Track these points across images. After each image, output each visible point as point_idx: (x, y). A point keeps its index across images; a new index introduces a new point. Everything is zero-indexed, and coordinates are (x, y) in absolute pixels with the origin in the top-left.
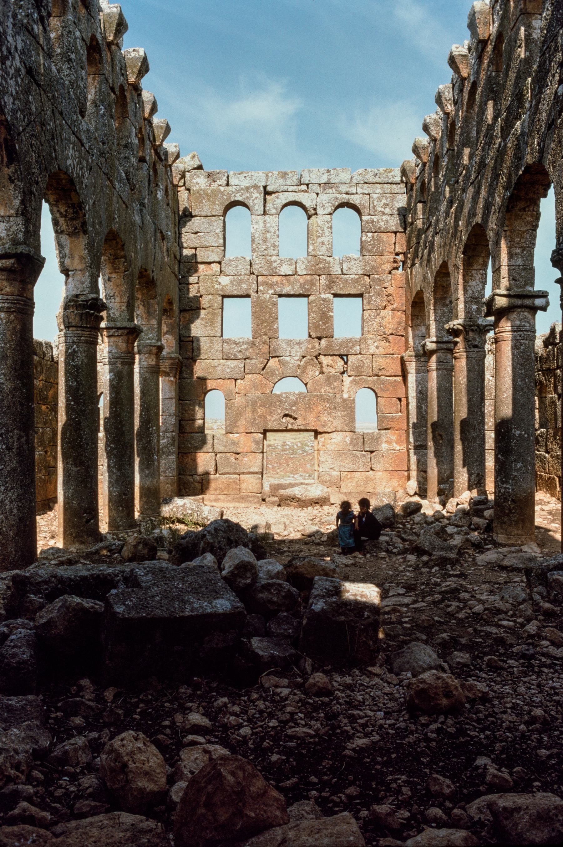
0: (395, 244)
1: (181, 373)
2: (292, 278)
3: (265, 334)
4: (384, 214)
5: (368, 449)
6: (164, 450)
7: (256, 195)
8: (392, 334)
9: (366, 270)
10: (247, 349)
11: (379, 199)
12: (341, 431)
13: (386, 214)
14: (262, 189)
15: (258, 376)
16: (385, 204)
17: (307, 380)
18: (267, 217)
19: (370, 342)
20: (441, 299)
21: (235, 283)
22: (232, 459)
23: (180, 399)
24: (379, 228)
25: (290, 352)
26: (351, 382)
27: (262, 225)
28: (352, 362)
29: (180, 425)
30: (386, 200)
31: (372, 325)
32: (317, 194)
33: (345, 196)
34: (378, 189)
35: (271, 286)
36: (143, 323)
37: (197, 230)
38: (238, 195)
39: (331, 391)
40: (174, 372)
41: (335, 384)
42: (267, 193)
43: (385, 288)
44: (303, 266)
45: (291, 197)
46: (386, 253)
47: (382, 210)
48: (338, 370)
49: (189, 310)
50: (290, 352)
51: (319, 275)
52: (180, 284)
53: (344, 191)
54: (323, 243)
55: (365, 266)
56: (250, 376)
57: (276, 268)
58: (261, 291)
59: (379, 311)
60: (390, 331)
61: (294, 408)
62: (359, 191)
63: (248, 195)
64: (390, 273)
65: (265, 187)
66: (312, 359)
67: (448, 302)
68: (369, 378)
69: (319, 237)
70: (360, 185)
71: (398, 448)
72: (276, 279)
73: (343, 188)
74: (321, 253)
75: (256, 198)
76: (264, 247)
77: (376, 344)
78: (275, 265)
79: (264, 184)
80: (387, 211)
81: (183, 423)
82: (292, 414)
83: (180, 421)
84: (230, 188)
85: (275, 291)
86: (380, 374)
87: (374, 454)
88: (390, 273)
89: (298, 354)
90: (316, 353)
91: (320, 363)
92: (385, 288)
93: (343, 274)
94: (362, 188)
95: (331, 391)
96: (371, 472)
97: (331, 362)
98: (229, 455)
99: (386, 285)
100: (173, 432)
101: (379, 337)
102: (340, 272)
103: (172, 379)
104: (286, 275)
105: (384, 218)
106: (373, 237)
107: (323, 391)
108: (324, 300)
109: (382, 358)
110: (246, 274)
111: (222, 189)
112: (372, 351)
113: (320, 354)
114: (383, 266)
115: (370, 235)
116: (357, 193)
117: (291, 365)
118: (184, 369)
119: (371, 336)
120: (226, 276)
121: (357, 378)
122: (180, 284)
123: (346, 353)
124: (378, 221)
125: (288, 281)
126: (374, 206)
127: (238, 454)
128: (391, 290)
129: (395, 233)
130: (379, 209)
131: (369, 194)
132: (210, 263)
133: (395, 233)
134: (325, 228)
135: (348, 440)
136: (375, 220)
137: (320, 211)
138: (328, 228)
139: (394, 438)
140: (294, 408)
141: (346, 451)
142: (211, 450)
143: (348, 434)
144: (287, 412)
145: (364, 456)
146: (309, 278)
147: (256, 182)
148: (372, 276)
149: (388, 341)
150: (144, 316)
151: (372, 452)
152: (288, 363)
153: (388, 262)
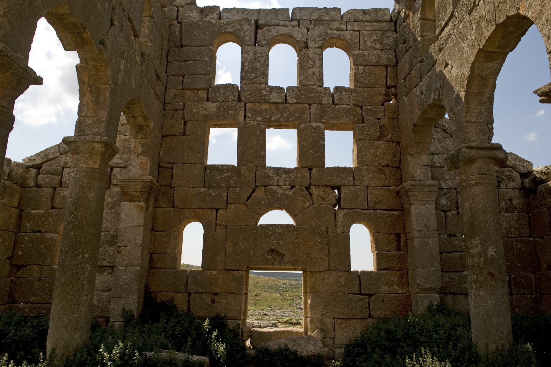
0: (386, 77)
1: (156, 200)
2: (281, 106)
3: (251, 162)
4: (375, 49)
5: (366, 292)
6: (125, 287)
7: (246, 27)
8: (388, 166)
9: (358, 101)
10: (230, 177)
11: (370, 35)
12: (335, 270)
13: (377, 49)
14: (253, 22)
15: (242, 207)
16: (374, 40)
17: (297, 212)
18: (257, 48)
19: (364, 172)
20: (478, 94)
21: (222, 109)
22: (209, 300)
23: (153, 230)
24: (370, 62)
25: (278, 181)
26: (345, 215)
27: (252, 55)
28: (345, 193)
29: (151, 258)
30: (377, 36)
31: (366, 155)
32: (308, 30)
33: (335, 32)
34: (368, 27)
35: (260, 113)
36: (89, 114)
37: (187, 58)
38: (229, 27)
39: (323, 225)
40: (145, 196)
41: (327, 217)
42: (257, 26)
43: (378, 119)
44: (294, 95)
45: (283, 30)
46: (378, 86)
47: (373, 45)
48: (330, 202)
49: (171, 135)
50: (278, 181)
51: (310, 105)
52: (164, 109)
53: (334, 27)
54: (314, 74)
55: (357, 96)
56: (233, 206)
57: (265, 95)
58: (249, 117)
59: (372, 141)
60: (386, 162)
61: (281, 242)
62: (349, 27)
63: (239, 27)
64: (383, 105)
65: (256, 22)
66: (302, 189)
67: (485, 99)
68: (364, 212)
69: (310, 67)
70: (351, 23)
71: (400, 291)
72: (265, 106)
73: (336, 25)
74: (312, 83)
75: (247, 30)
76: (254, 75)
77: (370, 176)
78: (264, 92)
79: (255, 18)
80: (378, 46)
81: (155, 256)
82: (280, 250)
83: (151, 254)
84: (222, 21)
85: (263, 118)
86: (376, 207)
87: (373, 298)
88: (383, 105)
89: (287, 183)
90: (306, 184)
91: (311, 194)
92: (378, 119)
93: (333, 104)
94: (352, 25)
95: (323, 225)
96: (370, 320)
97: (323, 193)
98: (204, 295)
99: (379, 116)
100: (137, 266)
101: (373, 169)
102: (331, 102)
103: (142, 204)
104: (275, 103)
105: (375, 52)
106: (364, 70)
107: (314, 224)
108: (315, 128)
109: (378, 190)
110: (233, 101)
111: (213, 21)
112: (366, 183)
113: (310, 185)
114: (375, 98)
115: (361, 68)
116: (347, 30)
117: (278, 195)
118: (160, 197)
119: (365, 167)
120: (213, 102)
121: (351, 211)
122: (164, 109)
123: (338, 184)
124: (369, 54)
125: (277, 109)
126: (365, 42)
127: (216, 294)
128: (384, 121)
129: (386, 67)
130: (370, 44)
131: (359, 31)
132: (198, 90)
133: (386, 67)
134: (316, 60)
135: (342, 281)
136: (366, 54)
137: (311, 44)
138: (319, 59)
139: (395, 279)
140: (281, 242)
141: (340, 294)
142: (184, 289)
143: (342, 273)
144: (273, 247)
145: (362, 300)
146: (299, 106)
147: (247, 16)
148: (364, 108)
149: (383, 172)
150: (91, 106)
151: (370, 295)
152: (275, 192)
153: (380, 94)
